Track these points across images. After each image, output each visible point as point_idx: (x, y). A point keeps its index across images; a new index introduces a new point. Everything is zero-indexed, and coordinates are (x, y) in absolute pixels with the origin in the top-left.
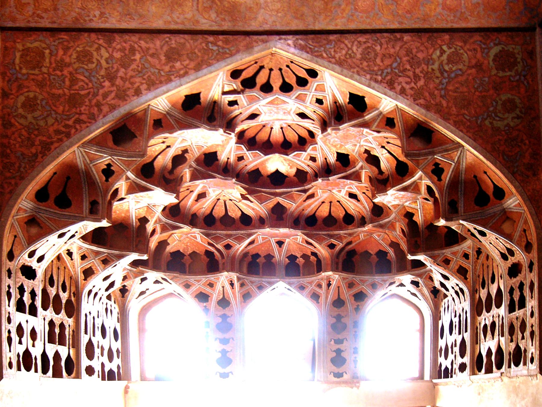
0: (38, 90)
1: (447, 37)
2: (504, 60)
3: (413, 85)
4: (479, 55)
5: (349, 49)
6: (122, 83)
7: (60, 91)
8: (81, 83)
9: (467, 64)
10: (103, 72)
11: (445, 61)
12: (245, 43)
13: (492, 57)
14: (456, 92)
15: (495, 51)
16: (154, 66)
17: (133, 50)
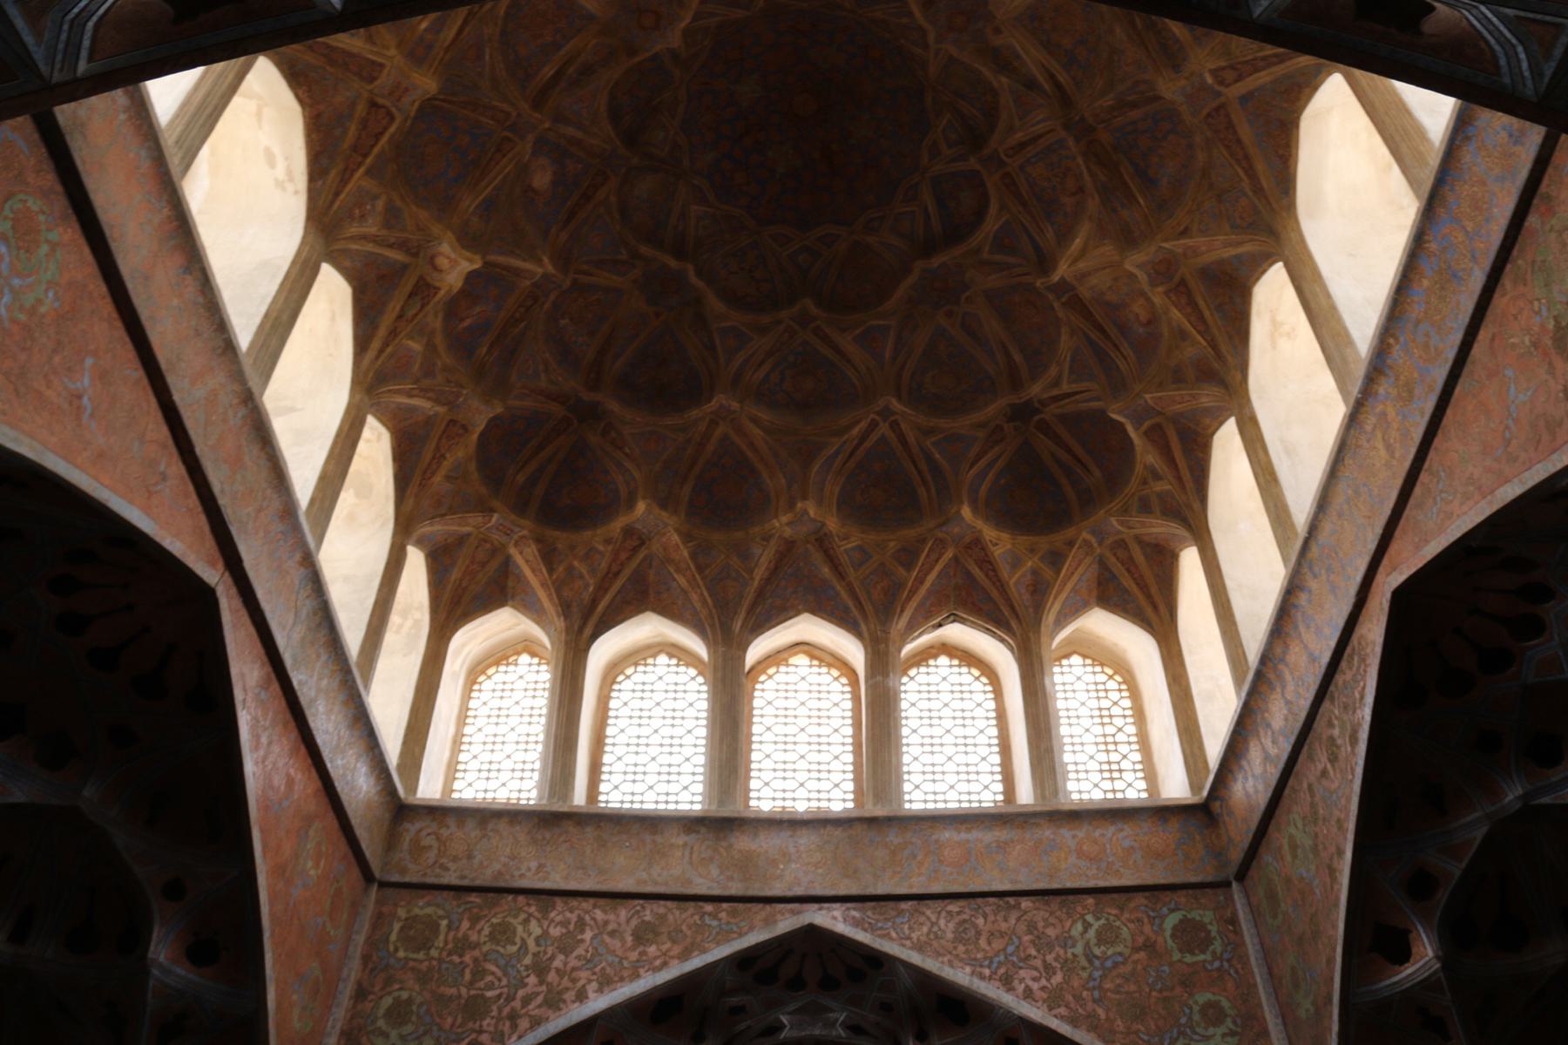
0: (417, 987)
1: (1090, 901)
2: (1191, 936)
3: (1044, 982)
4: (1147, 929)
5: (933, 924)
6: (557, 979)
7: (453, 991)
8: (489, 978)
9: (1129, 944)
10: (528, 960)
11: (1093, 941)
12: (763, 914)
13: (1168, 933)
14: (1118, 992)
15: (1172, 921)
16: (613, 952)
17: (581, 925)
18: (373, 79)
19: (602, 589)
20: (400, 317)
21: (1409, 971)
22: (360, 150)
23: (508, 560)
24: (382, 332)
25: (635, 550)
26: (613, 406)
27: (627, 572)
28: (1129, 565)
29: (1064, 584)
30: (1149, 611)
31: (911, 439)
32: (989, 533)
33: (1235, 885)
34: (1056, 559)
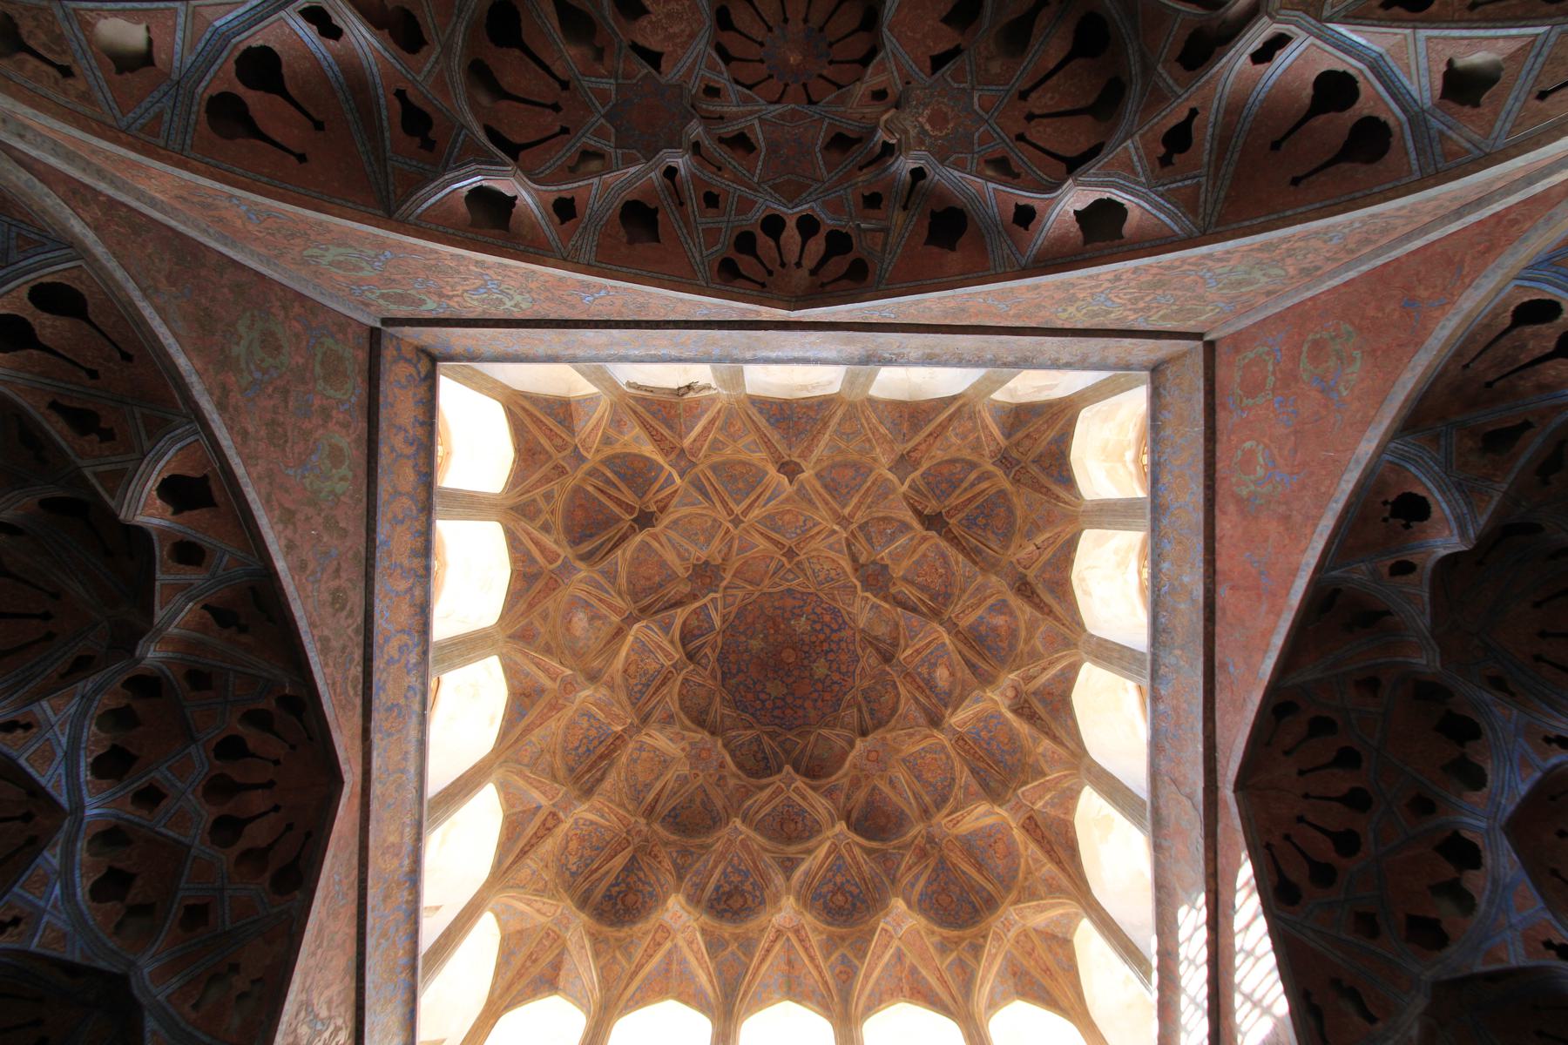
10: (1079, 303)
11: (506, 300)
18: (1030, 818)
19: (943, 427)
20: (1044, 669)
21: (150, 484)
22: (1045, 788)
23: (1008, 436)
24: (1059, 667)
25: (914, 449)
26: (916, 524)
27: (923, 434)
28: (551, 434)
29: (597, 425)
30: (528, 405)
31: (718, 505)
32: (659, 459)
33: (378, 325)
34: (607, 441)
